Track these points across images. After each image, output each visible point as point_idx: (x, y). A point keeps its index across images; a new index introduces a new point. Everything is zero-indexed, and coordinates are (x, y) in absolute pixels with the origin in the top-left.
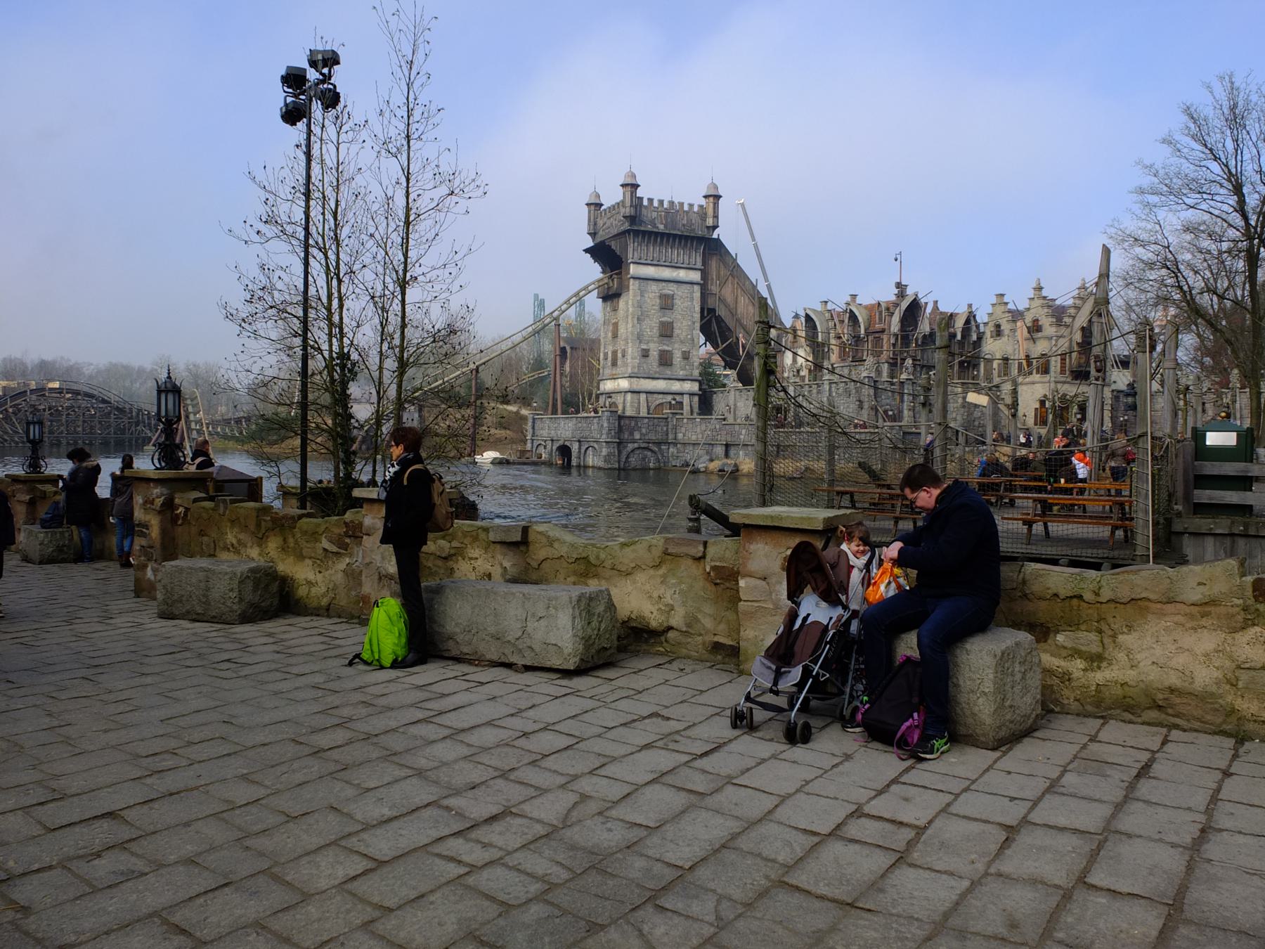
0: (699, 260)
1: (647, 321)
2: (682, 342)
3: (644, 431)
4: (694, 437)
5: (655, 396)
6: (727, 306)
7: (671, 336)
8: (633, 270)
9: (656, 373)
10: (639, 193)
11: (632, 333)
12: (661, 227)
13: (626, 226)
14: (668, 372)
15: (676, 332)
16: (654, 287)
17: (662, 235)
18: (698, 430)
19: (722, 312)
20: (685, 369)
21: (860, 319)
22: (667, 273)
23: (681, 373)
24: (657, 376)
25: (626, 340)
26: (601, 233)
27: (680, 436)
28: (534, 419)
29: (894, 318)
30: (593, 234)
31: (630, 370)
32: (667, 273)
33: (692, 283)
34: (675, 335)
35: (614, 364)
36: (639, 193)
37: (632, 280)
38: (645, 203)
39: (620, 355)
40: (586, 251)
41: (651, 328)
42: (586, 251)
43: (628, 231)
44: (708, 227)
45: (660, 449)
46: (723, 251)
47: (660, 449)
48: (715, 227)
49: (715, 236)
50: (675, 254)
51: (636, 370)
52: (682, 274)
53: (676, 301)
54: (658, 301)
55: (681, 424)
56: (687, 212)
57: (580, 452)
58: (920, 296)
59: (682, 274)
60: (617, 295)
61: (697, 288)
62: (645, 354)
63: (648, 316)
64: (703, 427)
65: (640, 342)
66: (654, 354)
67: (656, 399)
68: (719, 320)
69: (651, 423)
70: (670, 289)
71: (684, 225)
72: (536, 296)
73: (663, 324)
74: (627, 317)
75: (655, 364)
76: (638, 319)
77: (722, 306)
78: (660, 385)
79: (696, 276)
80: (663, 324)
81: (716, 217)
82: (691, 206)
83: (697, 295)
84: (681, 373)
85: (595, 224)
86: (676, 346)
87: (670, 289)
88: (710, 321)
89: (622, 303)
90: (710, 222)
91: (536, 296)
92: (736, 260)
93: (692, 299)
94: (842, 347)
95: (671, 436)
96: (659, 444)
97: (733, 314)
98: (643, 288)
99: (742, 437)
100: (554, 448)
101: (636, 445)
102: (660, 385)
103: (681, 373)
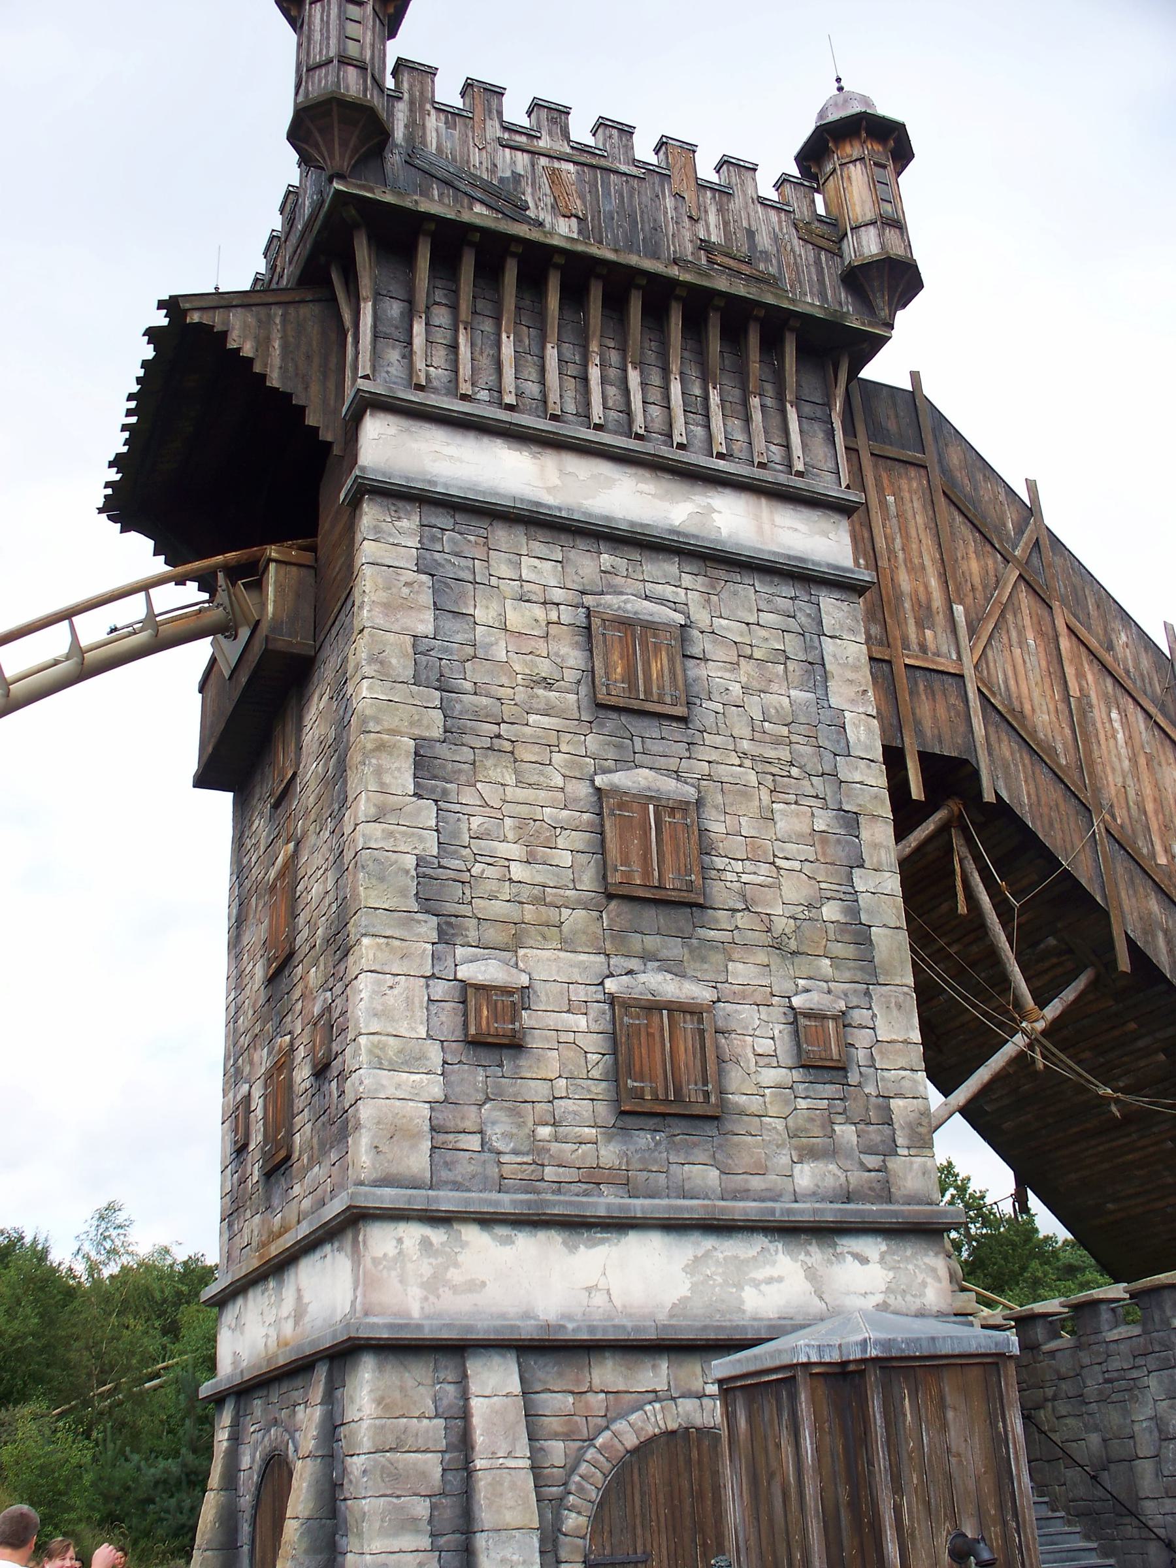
9: (594, 1178)
20: (830, 1152)
23: (806, 1176)
24: (607, 1201)
34: (721, 893)
46: (954, 458)
65: (447, 936)
77: (1007, 748)
86: (742, 972)
92: (1031, 512)
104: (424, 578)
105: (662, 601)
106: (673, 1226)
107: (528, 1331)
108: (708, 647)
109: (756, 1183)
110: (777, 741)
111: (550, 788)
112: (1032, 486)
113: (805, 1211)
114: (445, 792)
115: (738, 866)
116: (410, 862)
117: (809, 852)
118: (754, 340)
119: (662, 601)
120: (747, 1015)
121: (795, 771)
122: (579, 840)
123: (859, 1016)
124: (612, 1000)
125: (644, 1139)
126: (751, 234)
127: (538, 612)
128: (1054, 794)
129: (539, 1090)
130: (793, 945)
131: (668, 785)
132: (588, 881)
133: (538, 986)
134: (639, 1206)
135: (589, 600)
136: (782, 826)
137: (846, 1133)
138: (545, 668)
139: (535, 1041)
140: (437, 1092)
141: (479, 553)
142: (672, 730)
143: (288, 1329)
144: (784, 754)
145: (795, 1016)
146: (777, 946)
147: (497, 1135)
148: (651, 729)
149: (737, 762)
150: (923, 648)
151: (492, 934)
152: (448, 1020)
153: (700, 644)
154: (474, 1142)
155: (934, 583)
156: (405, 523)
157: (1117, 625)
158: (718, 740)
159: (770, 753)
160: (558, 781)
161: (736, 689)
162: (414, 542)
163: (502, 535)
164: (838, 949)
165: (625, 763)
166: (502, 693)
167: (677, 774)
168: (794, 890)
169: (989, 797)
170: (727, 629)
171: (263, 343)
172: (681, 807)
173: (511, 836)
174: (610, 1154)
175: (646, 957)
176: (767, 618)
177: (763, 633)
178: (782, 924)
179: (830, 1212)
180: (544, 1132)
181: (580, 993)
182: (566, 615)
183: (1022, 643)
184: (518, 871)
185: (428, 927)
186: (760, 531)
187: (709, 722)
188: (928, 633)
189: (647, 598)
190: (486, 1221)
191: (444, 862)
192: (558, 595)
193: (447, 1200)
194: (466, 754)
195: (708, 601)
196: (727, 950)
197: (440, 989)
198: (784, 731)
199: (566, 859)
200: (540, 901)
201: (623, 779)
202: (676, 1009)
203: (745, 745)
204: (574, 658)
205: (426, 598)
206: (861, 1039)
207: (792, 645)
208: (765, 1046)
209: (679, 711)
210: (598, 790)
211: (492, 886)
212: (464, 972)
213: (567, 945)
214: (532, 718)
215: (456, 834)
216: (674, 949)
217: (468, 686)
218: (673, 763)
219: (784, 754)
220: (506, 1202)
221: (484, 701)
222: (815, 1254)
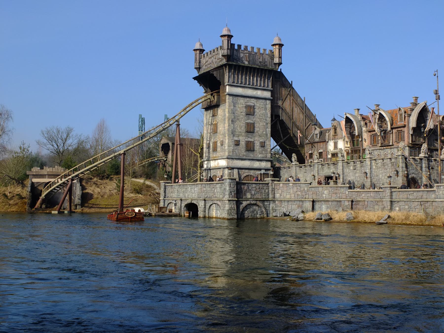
0: (270, 84)
2: (260, 136)
3: (253, 192)
4: (288, 196)
5: (243, 171)
6: (287, 113)
7: (253, 132)
8: (228, 89)
9: (244, 155)
10: (233, 41)
11: (228, 130)
12: (246, 63)
13: (224, 61)
14: (251, 155)
15: (256, 129)
16: (242, 101)
17: (247, 67)
18: (291, 191)
19: (284, 117)
20: (262, 153)
21: (387, 119)
22: (250, 92)
23: (260, 156)
24: (244, 157)
25: (224, 135)
26: (204, 67)
27: (277, 196)
28: (165, 186)
29: (411, 118)
30: (199, 69)
31: (227, 154)
32: (250, 92)
33: (265, 99)
34: (255, 131)
35: (215, 150)
36: (233, 41)
37: (227, 96)
38: (236, 47)
39: (219, 144)
40: (195, 78)
41: (241, 126)
42: (195, 78)
43: (225, 65)
44: (275, 64)
45: (264, 204)
46: (283, 79)
47: (264, 204)
48: (280, 64)
49: (279, 70)
50: (255, 80)
51: (231, 154)
52: (259, 93)
53: (256, 110)
54: (245, 110)
55: (278, 187)
56: (263, 54)
57: (205, 207)
58: (428, 104)
59: (259, 93)
60: (217, 106)
61: (268, 102)
62: (237, 144)
63: (238, 119)
64: (295, 189)
65: (234, 136)
66: (243, 143)
67: (244, 173)
68: (282, 122)
69: (258, 187)
70: (252, 102)
71: (260, 62)
72: (140, 116)
74: (225, 120)
75: (243, 150)
76: (232, 121)
77: (284, 114)
78: (247, 164)
79: (268, 94)
80: (248, 124)
81: (280, 57)
82: (265, 50)
83: (269, 106)
84: (260, 156)
85: (200, 62)
86: (256, 138)
87: (252, 102)
88: (276, 122)
89: (220, 111)
90: (276, 60)
91: (140, 116)
93: (266, 109)
94: (374, 138)
95: (271, 196)
96: (263, 201)
97: (291, 118)
98: (235, 101)
99: (324, 195)
100: (183, 205)
101: (248, 202)
102: (247, 164)
103: (260, 156)
105: (252, 103)
106: (249, 160)
107: (238, 167)
109: (256, 156)
112: (292, 82)
113: (259, 159)
117: (263, 127)
118: (264, 72)
119: (252, 103)
120: (256, 142)
122: (244, 127)
125: (247, 152)
126: (265, 59)
127: (242, 105)
128: (288, 118)
131: (251, 122)
134: (247, 158)
136: (261, 125)
137: (263, 152)
138: (242, 111)
139: (240, 145)
143: (216, 165)
148: (250, 116)
151: (237, 136)
152: (233, 143)
157: (298, 98)
159: (260, 117)
162: (231, 99)
163: (239, 98)
164: (264, 136)
165: (248, 120)
168: (261, 131)
171: (217, 75)
174: (245, 154)
178: (260, 134)
179: (262, 159)
181: (243, 141)
182: (244, 105)
183: (287, 101)
184: (239, 130)
190: (236, 159)
193: (233, 157)
199: (243, 129)
201: (247, 121)
202: (251, 142)
207: (264, 106)
208: (258, 145)
213: (243, 136)
216: (251, 136)
219: (262, 118)
220: (237, 157)
222: (260, 162)
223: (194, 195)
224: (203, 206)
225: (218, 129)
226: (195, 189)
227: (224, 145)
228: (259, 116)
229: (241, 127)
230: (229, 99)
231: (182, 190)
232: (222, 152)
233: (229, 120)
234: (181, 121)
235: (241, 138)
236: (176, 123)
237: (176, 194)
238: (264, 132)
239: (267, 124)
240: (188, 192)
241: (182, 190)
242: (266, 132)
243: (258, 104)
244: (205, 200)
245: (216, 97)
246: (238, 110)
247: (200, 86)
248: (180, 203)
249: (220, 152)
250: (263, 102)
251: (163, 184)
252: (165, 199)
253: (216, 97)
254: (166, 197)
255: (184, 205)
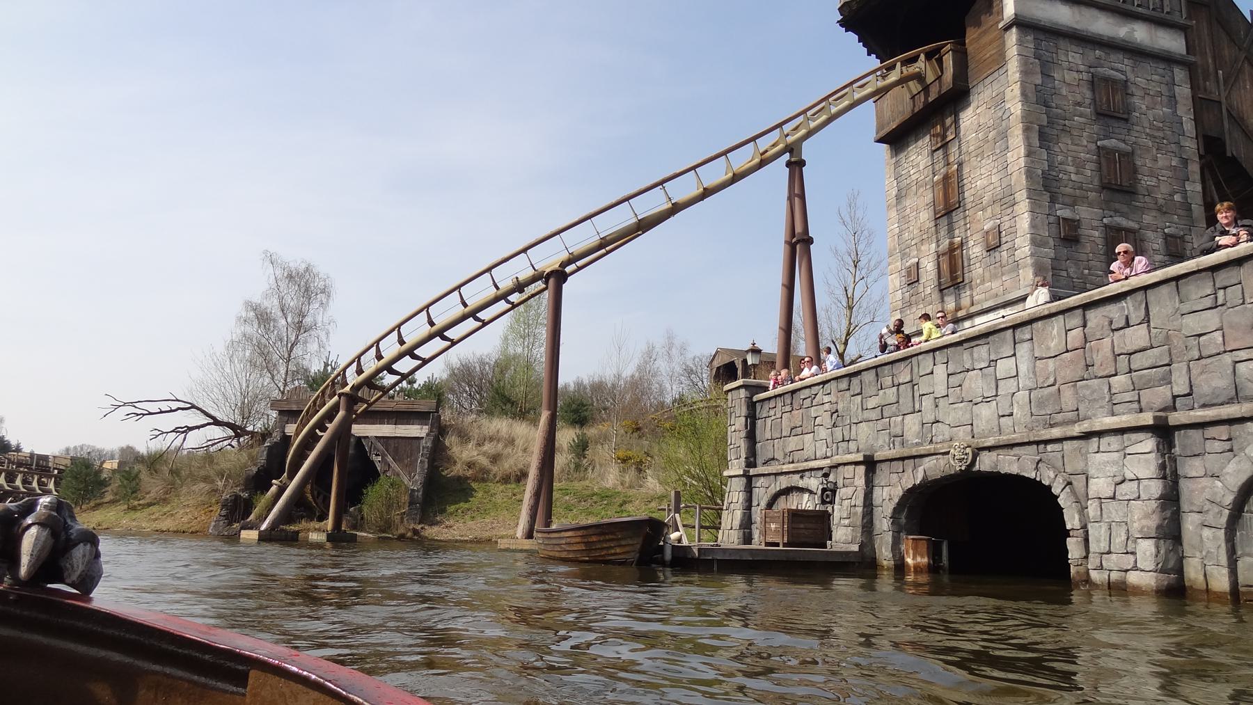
1: (1065, 144)
11: (1029, 173)
15: (1146, 181)
16: (1073, 57)
25: (1006, 201)
33: (1166, 59)
52: (1140, 33)
57: (1171, 499)
60: (957, 98)
63: (1064, 130)
65: (1053, 200)
70: (1117, 67)
73: (1104, 154)
74: (1004, 135)
76: (1042, 136)
86: (1147, 219)
87: (1117, 67)
100: (889, 493)
104: (1037, 61)
105: (1117, 70)
108: (1134, 90)
110: (1159, 129)
111: (1082, 146)
114: (1049, 146)
115: (1146, 178)
116: (1040, 172)
117: (1170, 174)
119: (1117, 70)
120: (1150, 234)
121: (1165, 141)
122: (1093, 166)
123: (1188, 238)
124: (1106, 226)
127: (1075, 75)
129: (1083, 257)
130: (1164, 209)
131: (1122, 145)
132: (1096, 182)
133: (1082, 220)
135: (1092, 70)
136: (1160, 163)
138: (1079, 98)
140: (1052, 255)
141: (1054, 50)
142: (1122, 124)
144: (1160, 134)
145: (1167, 237)
146: (1159, 210)
147: (1072, 270)
149: (1145, 137)
150: (1205, 90)
151: (1067, 200)
152: (1054, 229)
153: (1133, 89)
154: (1064, 273)
155: (1210, 61)
156: (1029, 38)
158: (1138, 128)
159: (1156, 134)
160: (1085, 143)
161: (1144, 107)
163: (1063, 43)
164: (1180, 212)
165: (1107, 137)
166: (1066, 108)
167: (1124, 141)
168: (1165, 189)
169: (1229, 154)
170: (1141, 82)
172: (1123, 154)
173: (1071, 164)
175: (1116, 211)
176: (1156, 77)
177: (1153, 84)
178: (1161, 202)
180: (1086, 272)
181: (1095, 223)
182: (1085, 76)
183: (1245, 88)
184: (1073, 177)
185: (1047, 196)
186: (1151, 38)
187: (1135, 120)
188: (1208, 83)
189: (1112, 69)
191: (1051, 173)
192: (1082, 68)
194: (1055, 132)
195: (1133, 70)
196: (1142, 210)
197: (1052, 219)
198: (1161, 125)
199: (1089, 173)
200: (1081, 188)
201: (1106, 143)
203: (1148, 130)
204: (1088, 94)
205: (1038, 69)
206: (1189, 246)
207: (1164, 89)
208: (1156, 246)
209: (1125, 116)
210: (1098, 147)
211: (1066, 182)
212: (1059, 213)
213: (1091, 205)
214: (1076, 118)
215: (1053, 162)
216: (1125, 208)
217: (1054, 105)
218: (1122, 137)
219: (1160, 134)
221: (1060, 111)
223: (986, 413)
224: (1156, 488)
225: (966, 188)
226: (1005, 367)
227: (1004, 247)
228: (1152, 126)
229: (1080, 166)
230: (1020, 43)
231: (872, 403)
232: (994, 277)
233: (1027, 130)
234: (808, 151)
235: (1084, 213)
236: (787, 156)
237: (823, 433)
238: (1177, 197)
239: (1185, 162)
240: (927, 403)
241: (872, 403)
242: (1185, 197)
243: (1143, 79)
244: (1163, 432)
245: (948, 60)
246: (1064, 92)
247: (869, 54)
248: (860, 482)
249: (983, 282)
250: (1160, 71)
251: (743, 393)
252: (752, 471)
253: (948, 60)
254: (760, 461)
255: (898, 492)
